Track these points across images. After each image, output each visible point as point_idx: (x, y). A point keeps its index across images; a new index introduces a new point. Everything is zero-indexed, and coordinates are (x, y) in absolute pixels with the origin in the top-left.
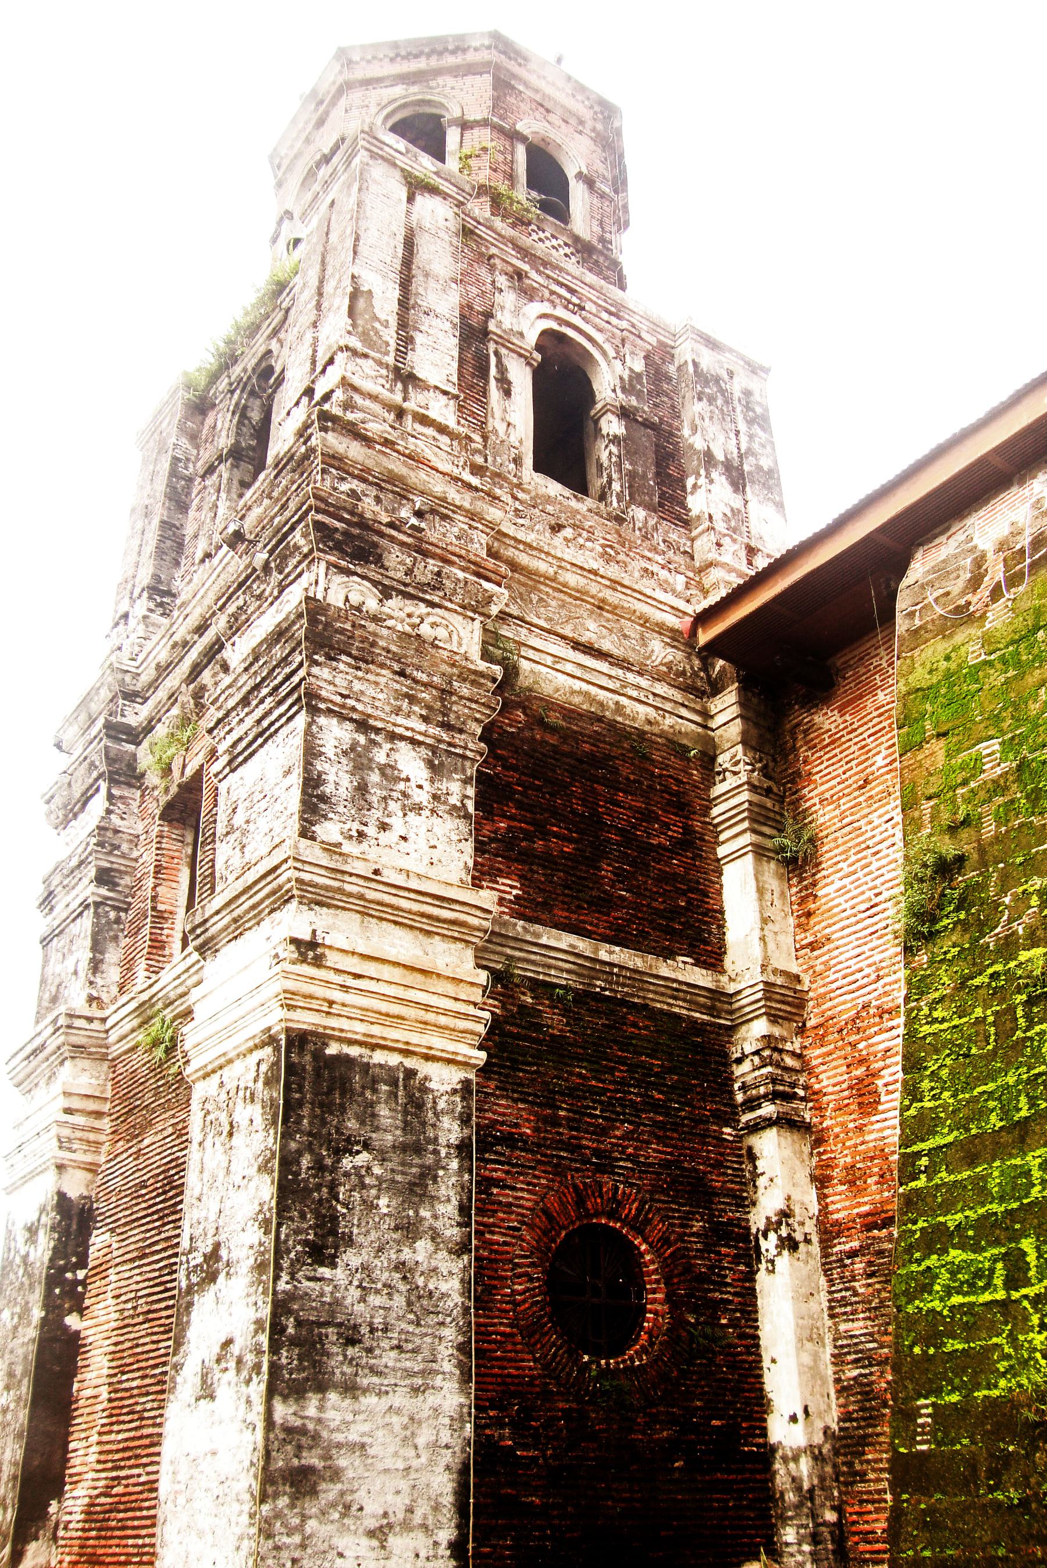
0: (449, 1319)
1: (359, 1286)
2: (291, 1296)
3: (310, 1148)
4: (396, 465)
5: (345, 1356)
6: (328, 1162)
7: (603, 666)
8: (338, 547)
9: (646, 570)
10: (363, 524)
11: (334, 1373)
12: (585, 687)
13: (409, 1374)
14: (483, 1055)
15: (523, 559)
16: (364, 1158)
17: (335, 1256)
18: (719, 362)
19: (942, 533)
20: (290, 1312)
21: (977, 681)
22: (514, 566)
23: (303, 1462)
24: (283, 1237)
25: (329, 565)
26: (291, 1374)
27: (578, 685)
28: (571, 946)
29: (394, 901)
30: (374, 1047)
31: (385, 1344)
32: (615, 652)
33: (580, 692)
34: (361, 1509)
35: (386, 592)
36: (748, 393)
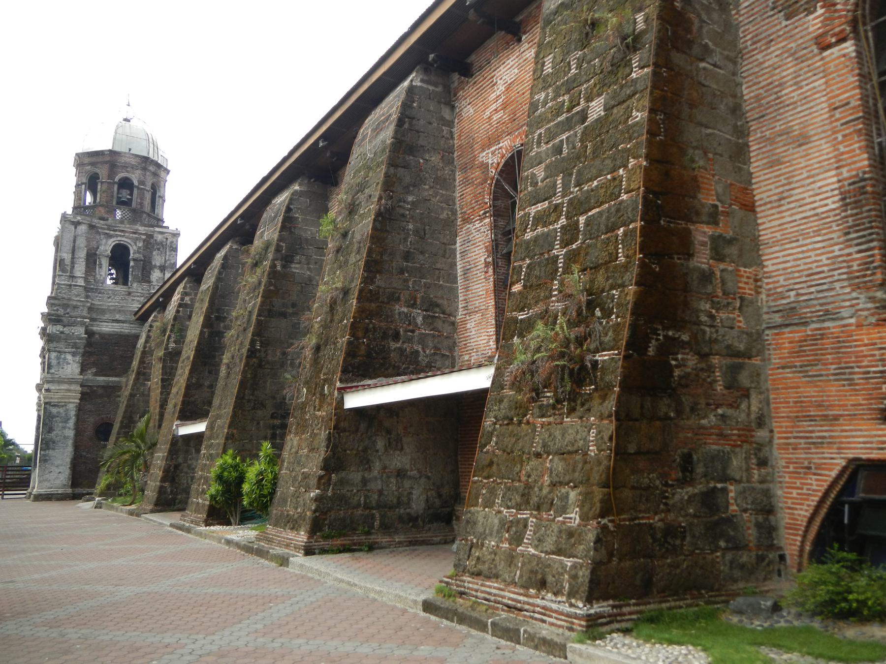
4: (65, 302)
10: (58, 316)
35: (64, 326)
36: (172, 242)
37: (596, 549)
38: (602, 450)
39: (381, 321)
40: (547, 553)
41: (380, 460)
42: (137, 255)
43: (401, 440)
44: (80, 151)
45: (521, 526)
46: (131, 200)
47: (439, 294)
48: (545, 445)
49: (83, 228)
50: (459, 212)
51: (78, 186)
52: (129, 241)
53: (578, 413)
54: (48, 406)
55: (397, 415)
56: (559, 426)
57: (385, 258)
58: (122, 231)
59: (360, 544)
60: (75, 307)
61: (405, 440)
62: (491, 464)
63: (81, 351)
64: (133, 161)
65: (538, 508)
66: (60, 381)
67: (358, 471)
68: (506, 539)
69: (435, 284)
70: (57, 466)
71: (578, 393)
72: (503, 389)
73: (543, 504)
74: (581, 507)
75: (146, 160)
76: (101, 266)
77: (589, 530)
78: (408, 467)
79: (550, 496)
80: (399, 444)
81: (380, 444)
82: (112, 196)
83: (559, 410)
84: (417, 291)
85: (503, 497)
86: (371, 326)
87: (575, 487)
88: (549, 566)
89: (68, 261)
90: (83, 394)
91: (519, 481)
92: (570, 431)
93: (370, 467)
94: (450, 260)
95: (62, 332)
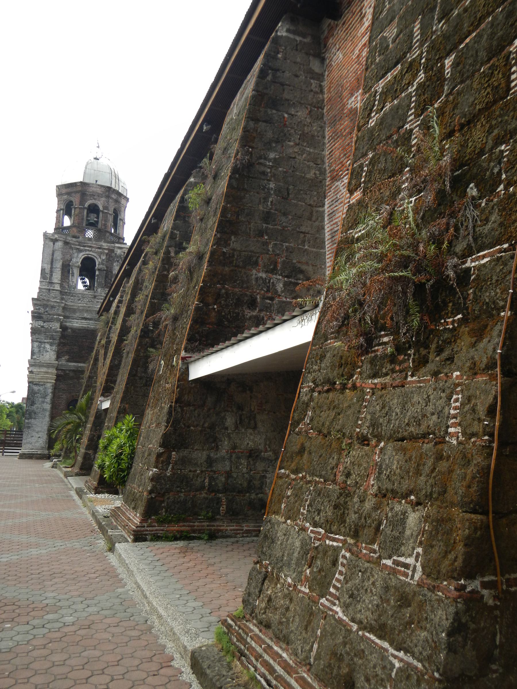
4: (45, 303)
10: (40, 313)
35: (44, 322)
37: (451, 648)
38: (473, 435)
39: (234, 287)
40: (363, 627)
41: (230, 438)
42: (101, 266)
43: (255, 418)
44: (60, 183)
45: (328, 561)
46: (97, 222)
47: (304, 259)
48: (374, 424)
49: (59, 244)
50: (328, 171)
51: (58, 211)
52: (95, 255)
53: (431, 367)
55: (251, 390)
56: (398, 390)
57: (242, 218)
58: (90, 247)
59: (200, 531)
60: (53, 307)
61: (258, 417)
62: (302, 451)
63: (57, 342)
64: (99, 190)
65: (356, 535)
66: (41, 365)
67: (203, 450)
68: (307, 579)
69: (299, 249)
70: (37, 432)
71: (432, 331)
72: (326, 340)
73: (364, 527)
74: (428, 547)
75: (109, 189)
76: (73, 276)
77: (440, 600)
78: (261, 447)
79: (375, 515)
80: (252, 422)
81: (230, 421)
82: (83, 219)
83: (401, 363)
84: (278, 255)
85: (310, 505)
86: (223, 291)
87: (418, 504)
88: (361, 654)
89: (48, 271)
90: (58, 376)
91: (334, 481)
92: (416, 398)
93: (217, 447)
94: (317, 223)
95: (42, 327)
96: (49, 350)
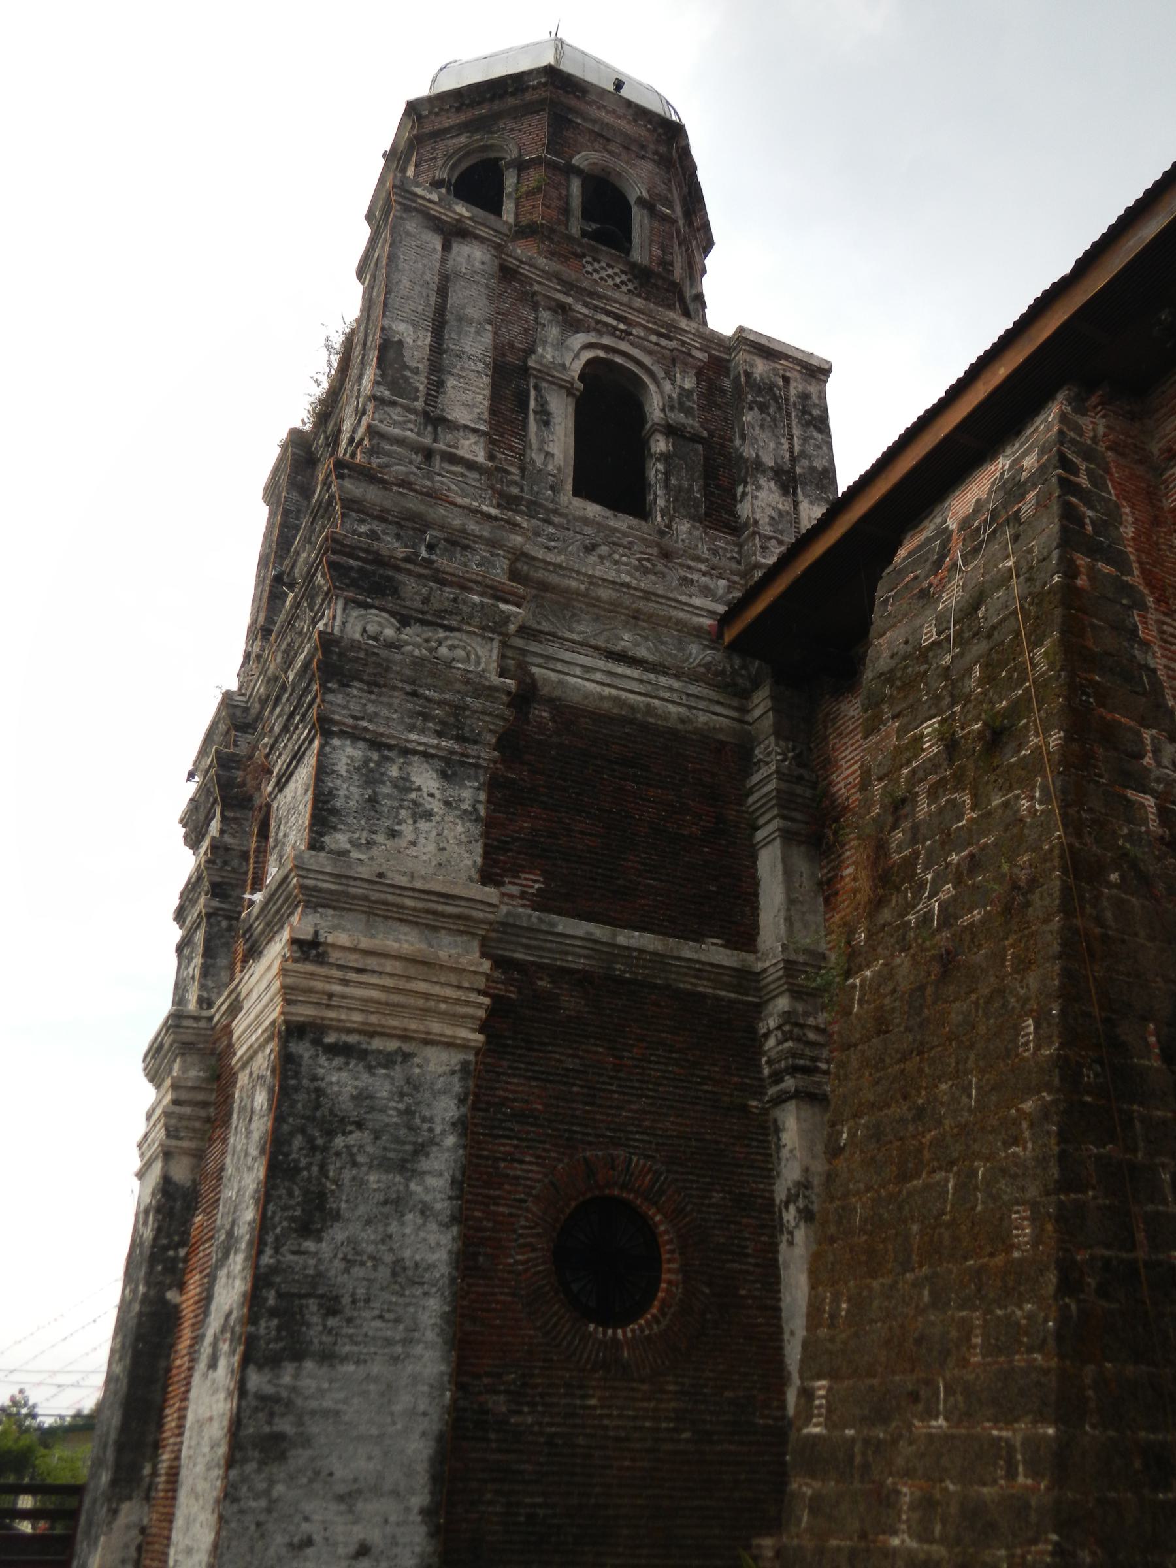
0: (434, 1290)
1: (344, 1259)
2: (274, 1270)
3: (303, 1131)
4: (413, 504)
5: (325, 1326)
6: (320, 1142)
7: (635, 673)
8: (354, 584)
9: (685, 579)
10: (379, 560)
11: (311, 1342)
12: (614, 692)
13: (389, 1342)
14: (481, 1038)
15: (554, 579)
16: (355, 1137)
17: (320, 1231)
18: (774, 369)
19: (926, 517)
20: (270, 1285)
21: (926, 662)
22: (544, 586)
23: (276, 1429)
24: (269, 1214)
25: (347, 601)
26: (268, 1344)
27: (607, 691)
28: (587, 933)
29: (399, 900)
30: (372, 1035)
31: (367, 1314)
32: (650, 657)
33: (610, 698)
34: (331, 1474)
36: (805, 396)
52: (647, 360)
54: (303, 1049)
60: (457, 542)
70: (347, 1498)
76: (545, 421)
96: (436, 806)
